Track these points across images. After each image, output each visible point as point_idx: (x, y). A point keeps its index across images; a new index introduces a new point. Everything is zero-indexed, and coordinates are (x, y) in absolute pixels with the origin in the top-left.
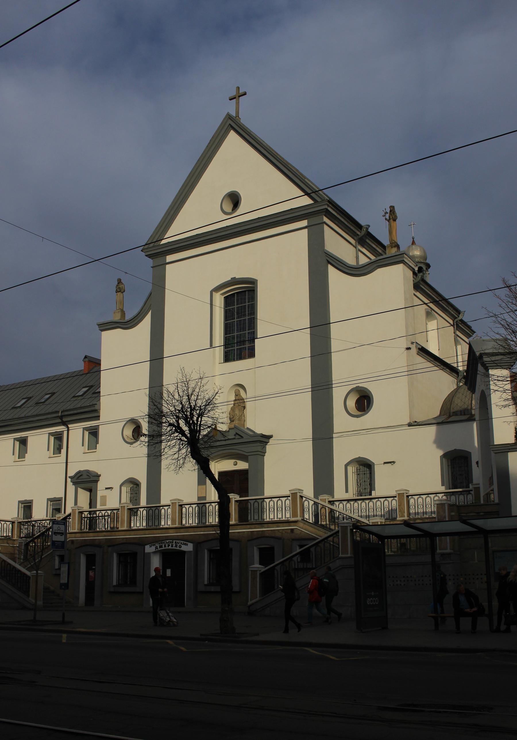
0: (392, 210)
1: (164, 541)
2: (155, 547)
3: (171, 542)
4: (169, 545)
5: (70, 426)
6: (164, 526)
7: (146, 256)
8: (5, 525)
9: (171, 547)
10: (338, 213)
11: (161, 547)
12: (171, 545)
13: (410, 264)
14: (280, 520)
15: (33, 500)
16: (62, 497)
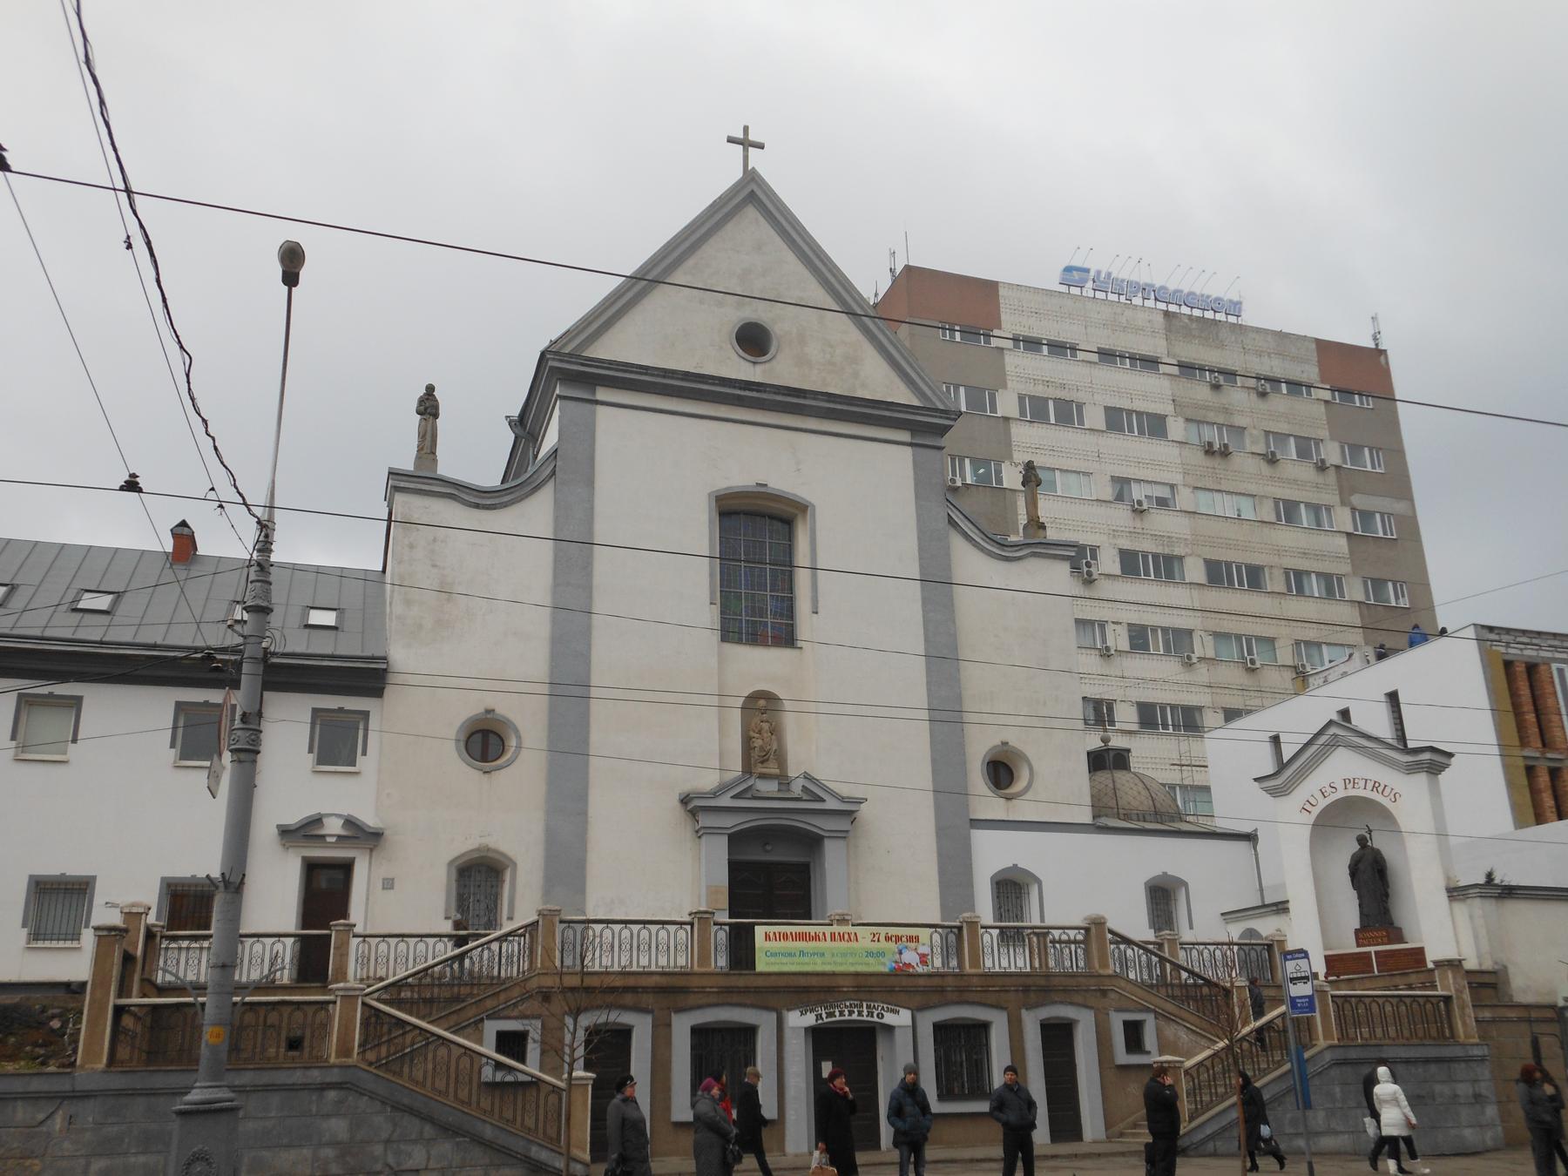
4: (850, 1014)
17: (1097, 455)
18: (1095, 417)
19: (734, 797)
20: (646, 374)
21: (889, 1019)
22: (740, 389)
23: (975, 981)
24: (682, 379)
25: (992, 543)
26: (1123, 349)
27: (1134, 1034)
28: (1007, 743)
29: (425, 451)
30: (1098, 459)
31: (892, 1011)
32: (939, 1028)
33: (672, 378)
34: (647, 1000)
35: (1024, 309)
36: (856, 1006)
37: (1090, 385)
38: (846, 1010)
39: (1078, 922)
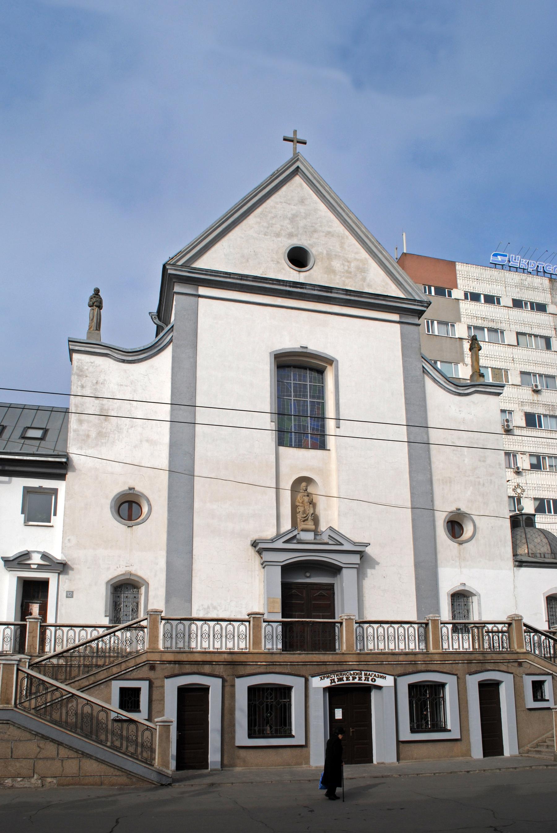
1: (346, 672)
2: (331, 680)
3: (357, 674)
4: (354, 678)
6: (384, 651)
9: (359, 680)
11: (340, 680)
12: (358, 677)
14: (412, 652)
17: (512, 359)
18: (511, 338)
19: (284, 542)
21: (379, 682)
23: (437, 657)
25: (451, 384)
26: (527, 300)
27: (538, 686)
28: (460, 509)
29: (92, 329)
30: (512, 362)
31: (381, 677)
32: (411, 687)
34: (220, 670)
35: (470, 277)
36: (357, 674)
37: (508, 320)
38: (351, 677)
39: (504, 619)
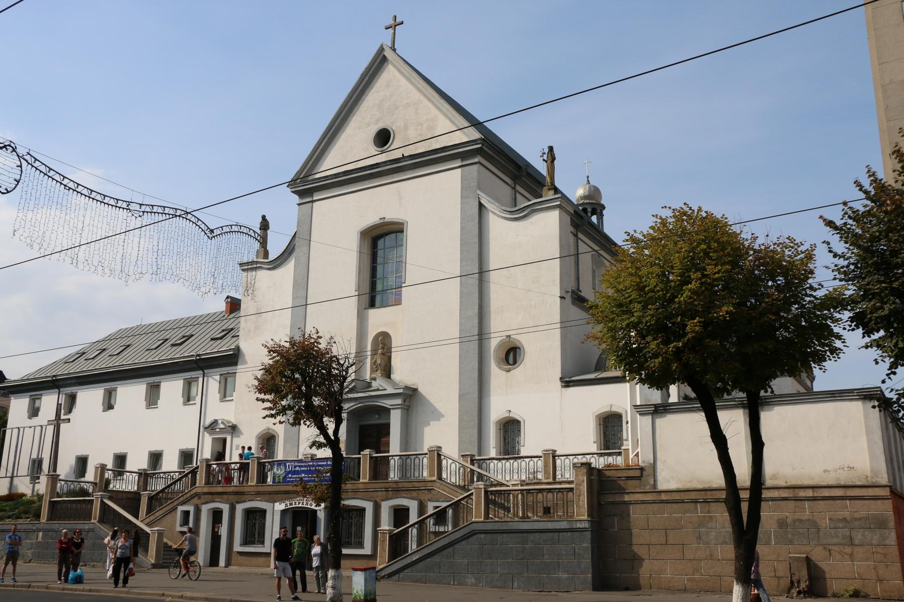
0: (551, 149)
4: (299, 503)
5: (206, 371)
7: (293, 192)
8: (131, 477)
10: (494, 152)
11: (291, 504)
13: (568, 208)
15: (127, 453)
16: (194, 449)
20: (328, 180)
22: (369, 170)
24: (344, 176)
33: (339, 177)
